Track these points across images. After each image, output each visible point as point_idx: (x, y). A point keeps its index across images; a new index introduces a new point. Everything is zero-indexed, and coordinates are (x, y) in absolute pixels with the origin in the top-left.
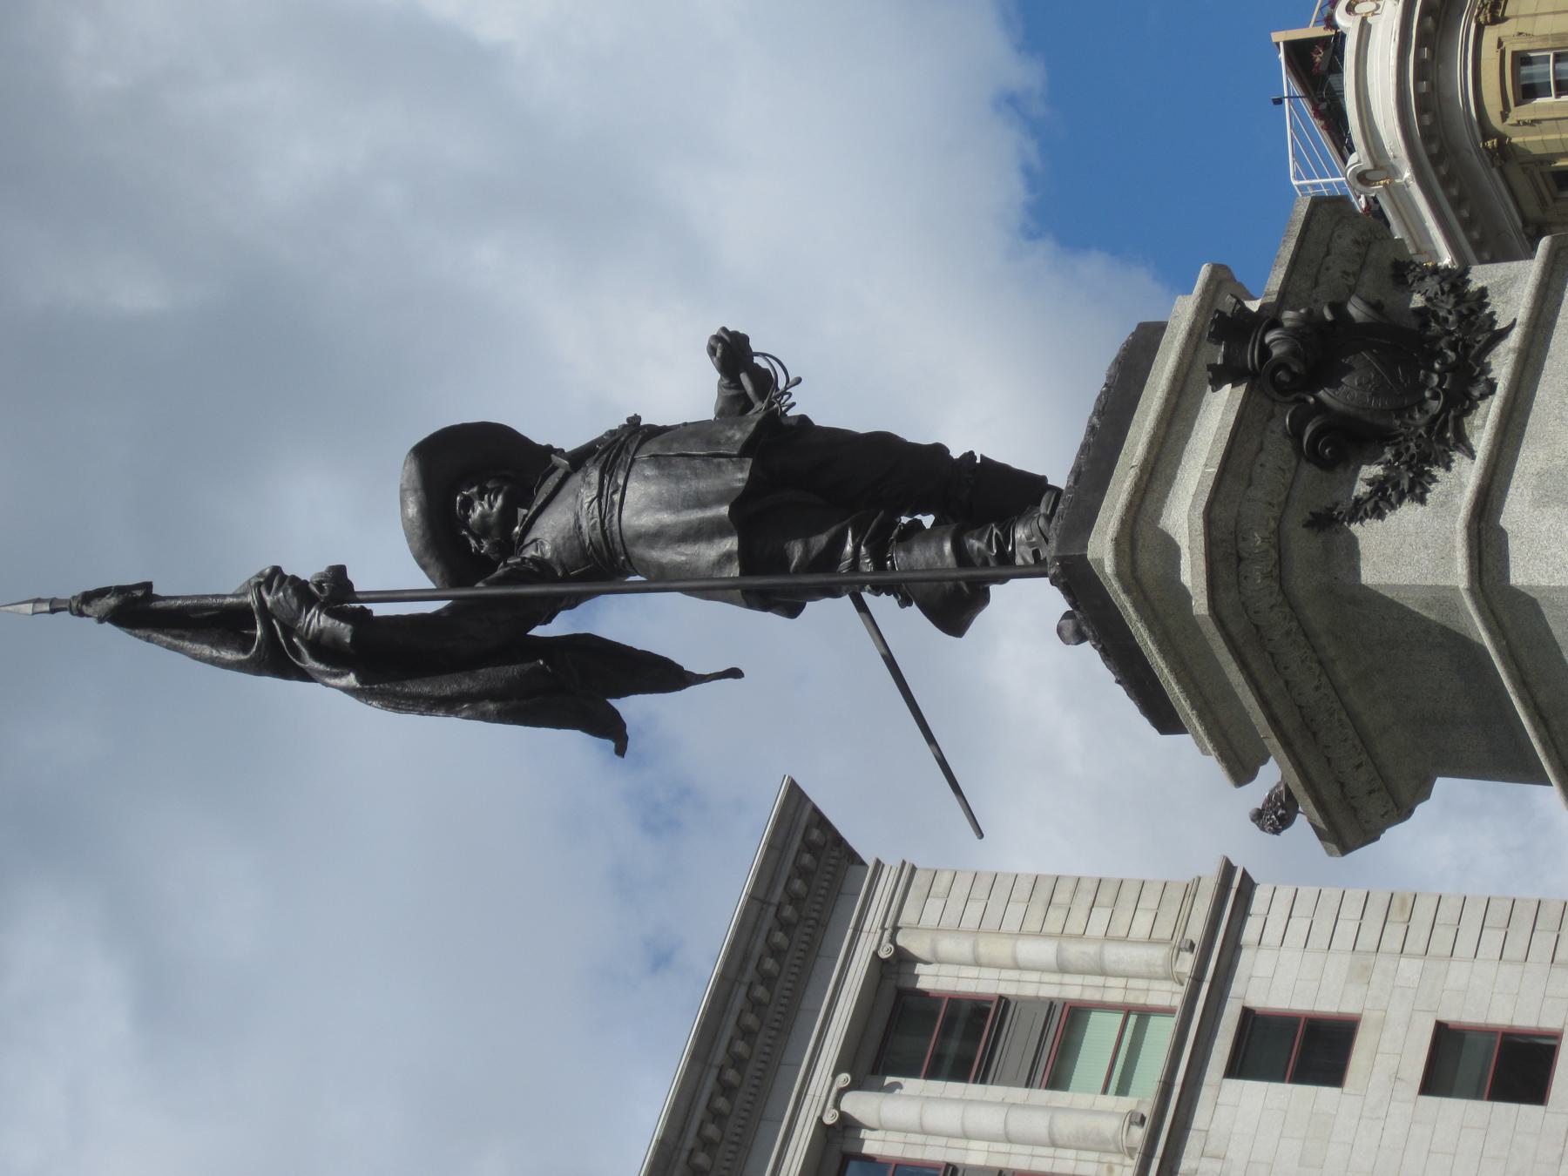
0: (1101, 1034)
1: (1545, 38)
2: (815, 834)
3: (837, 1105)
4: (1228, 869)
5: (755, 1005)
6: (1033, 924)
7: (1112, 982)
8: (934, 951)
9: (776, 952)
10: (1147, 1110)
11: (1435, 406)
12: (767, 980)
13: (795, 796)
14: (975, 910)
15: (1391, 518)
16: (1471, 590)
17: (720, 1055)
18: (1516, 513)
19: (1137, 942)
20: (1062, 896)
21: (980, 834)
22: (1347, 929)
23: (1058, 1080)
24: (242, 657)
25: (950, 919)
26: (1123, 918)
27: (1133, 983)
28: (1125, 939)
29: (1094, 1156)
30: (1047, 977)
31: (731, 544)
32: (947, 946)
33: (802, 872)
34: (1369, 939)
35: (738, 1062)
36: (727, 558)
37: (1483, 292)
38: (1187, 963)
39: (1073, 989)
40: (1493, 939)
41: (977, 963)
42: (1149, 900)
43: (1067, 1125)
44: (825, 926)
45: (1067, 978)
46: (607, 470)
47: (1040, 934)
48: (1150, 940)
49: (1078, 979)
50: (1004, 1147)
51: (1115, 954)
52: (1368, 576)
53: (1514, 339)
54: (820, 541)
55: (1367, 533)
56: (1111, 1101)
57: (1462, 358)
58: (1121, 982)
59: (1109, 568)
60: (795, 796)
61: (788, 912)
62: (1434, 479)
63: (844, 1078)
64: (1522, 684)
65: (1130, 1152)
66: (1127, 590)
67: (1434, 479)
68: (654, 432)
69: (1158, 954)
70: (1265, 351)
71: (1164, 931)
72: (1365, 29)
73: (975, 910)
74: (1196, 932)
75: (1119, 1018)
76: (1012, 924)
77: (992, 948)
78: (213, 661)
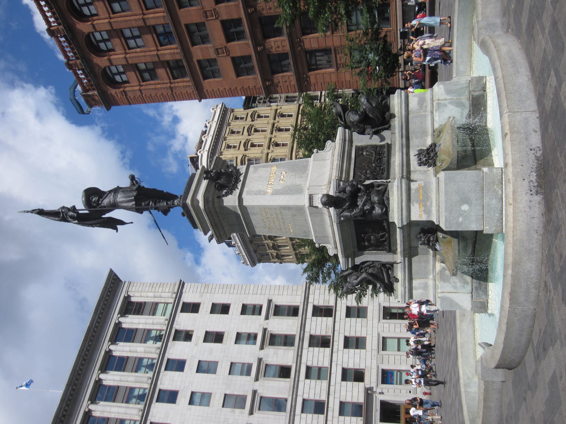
0: (161, 307)
1: (228, 158)
2: (115, 277)
3: (118, 319)
4: (181, 281)
5: (105, 304)
6: (150, 290)
7: (162, 299)
8: (134, 295)
9: (108, 296)
10: (168, 318)
11: (233, 183)
12: (107, 300)
13: (111, 271)
14: (141, 288)
15: (228, 197)
16: (238, 206)
17: (99, 312)
18: (244, 196)
19: (167, 293)
20: (155, 286)
21: (168, 244)
22: (199, 289)
23: (154, 314)
24: (59, 219)
25: (137, 290)
26: (164, 289)
27: (166, 299)
28: (165, 292)
29: (160, 326)
30: (152, 298)
31: (134, 203)
32: (136, 294)
33: (112, 283)
34: (202, 291)
35: (102, 313)
36: (133, 205)
37: (239, 169)
38: (174, 295)
39: (156, 300)
40: (221, 290)
41: (141, 297)
42: (169, 286)
43: (155, 321)
44: (116, 292)
45: (155, 299)
46: (115, 193)
47: (151, 292)
48: (169, 292)
49: (157, 299)
50: (145, 325)
51: (163, 295)
52: (225, 204)
53: (243, 175)
54: (147, 202)
55: (225, 199)
56: (162, 317)
57: (237, 177)
58: (164, 299)
59: (190, 204)
60: (111, 271)
61: (110, 289)
62: (233, 192)
63: (119, 315)
64: (244, 219)
65: (165, 325)
66: (192, 207)
67: (233, 192)
68: (121, 188)
69: (170, 294)
70: (211, 175)
71: (171, 291)
72: (202, 155)
73: (141, 288)
74: (176, 290)
75: (164, 304)
76: (147, 290)
77: (143, 294)
78: (54, 220)
